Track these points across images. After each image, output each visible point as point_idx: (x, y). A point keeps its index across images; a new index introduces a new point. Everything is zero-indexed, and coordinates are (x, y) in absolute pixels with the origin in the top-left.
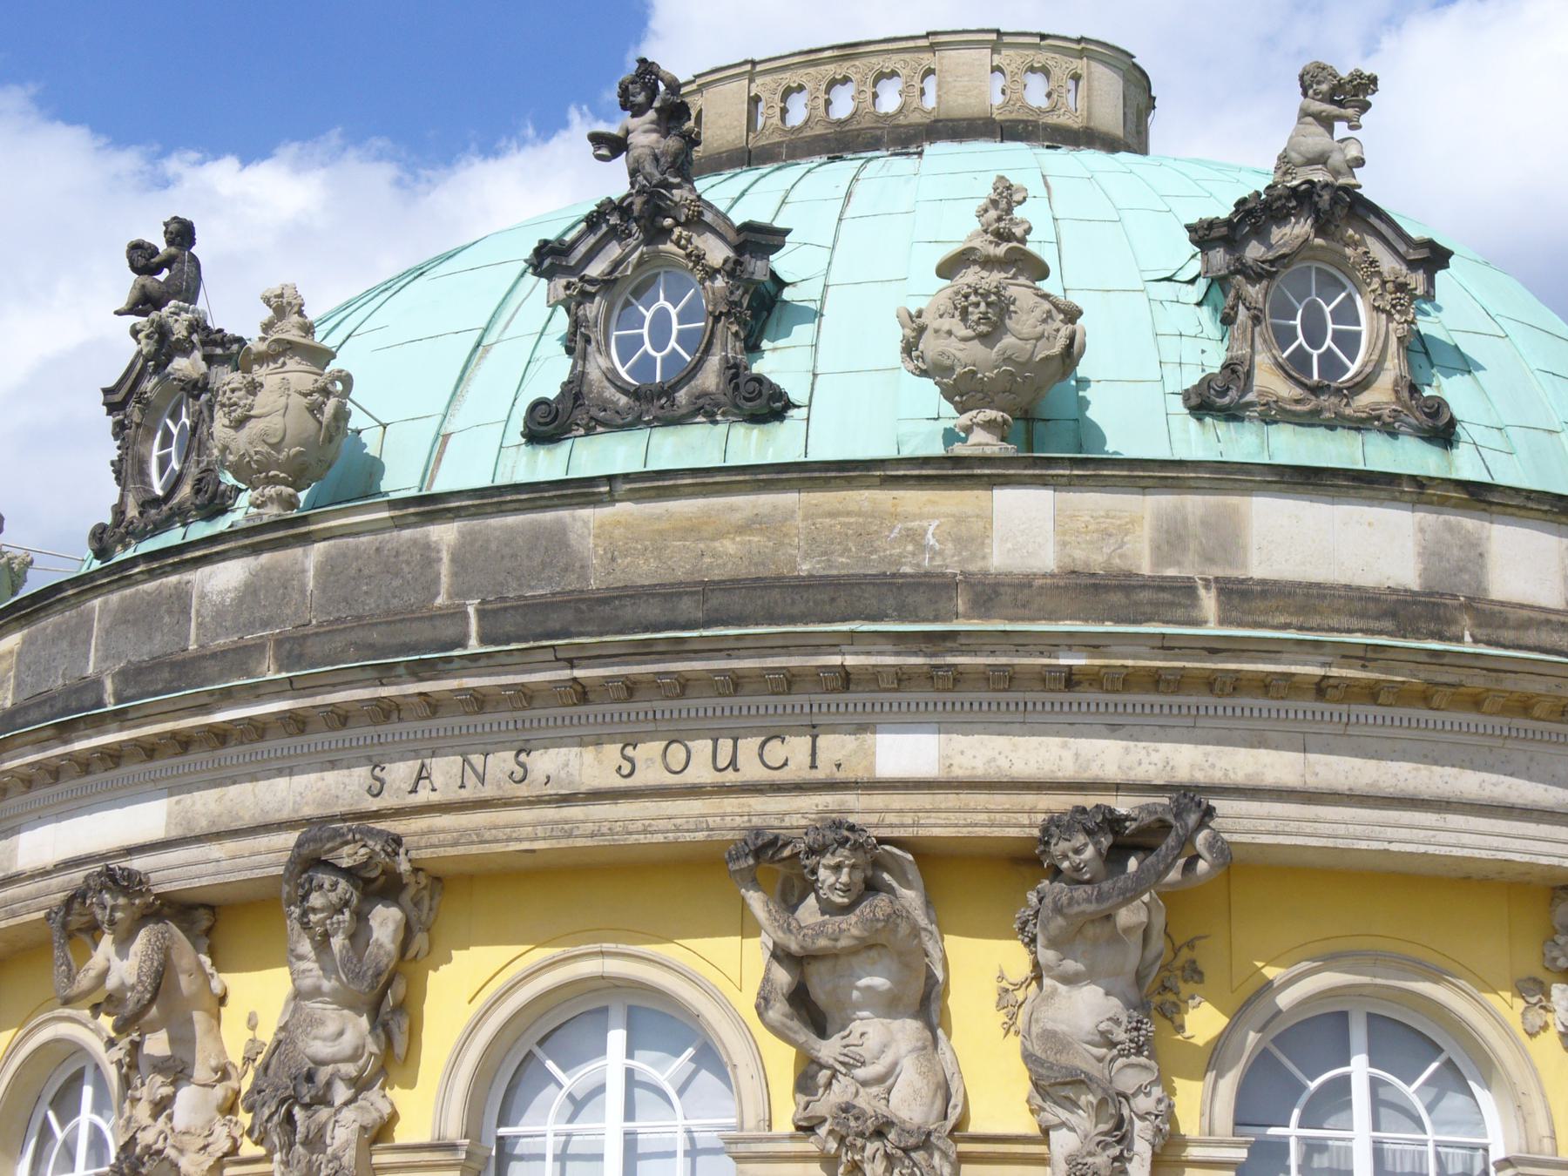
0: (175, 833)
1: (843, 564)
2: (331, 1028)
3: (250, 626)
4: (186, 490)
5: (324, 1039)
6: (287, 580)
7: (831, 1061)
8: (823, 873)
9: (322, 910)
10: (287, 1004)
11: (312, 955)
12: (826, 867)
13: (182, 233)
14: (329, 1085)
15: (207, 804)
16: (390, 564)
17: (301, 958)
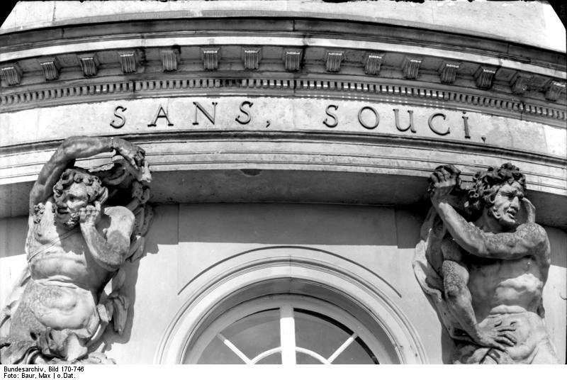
2: (66, 299)
5: (61, 308)
7: (492, 341)
8: (501, 200)
9: (80, 198)
10: (15, 289)
11: (58, 241)
12: (504, 194)
14: (67, 341)
17: (45, 242)
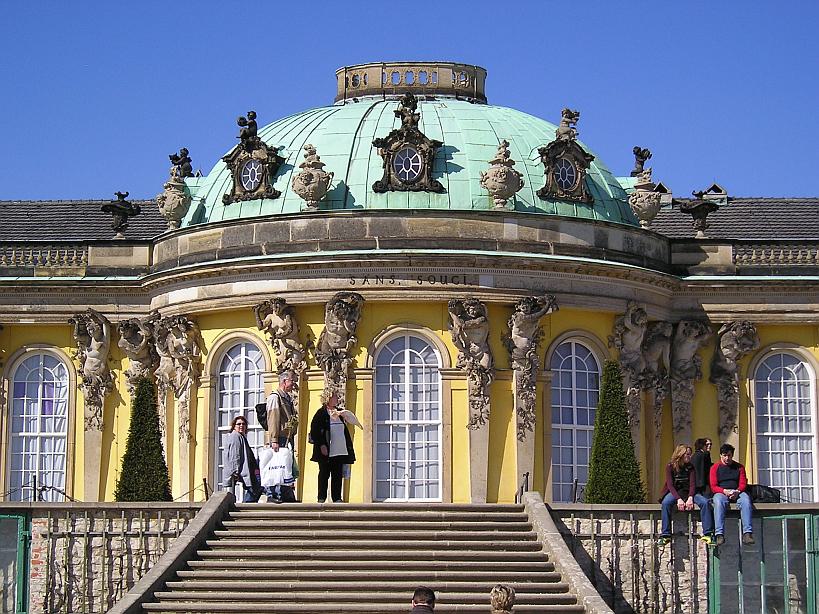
0: (290, 290)
1: (469, 235)
3: (310, 237)
4: (261, 189)
6: (321, 227)
13: (253, 116)
15: (300, 283)
16: (352, 226)
